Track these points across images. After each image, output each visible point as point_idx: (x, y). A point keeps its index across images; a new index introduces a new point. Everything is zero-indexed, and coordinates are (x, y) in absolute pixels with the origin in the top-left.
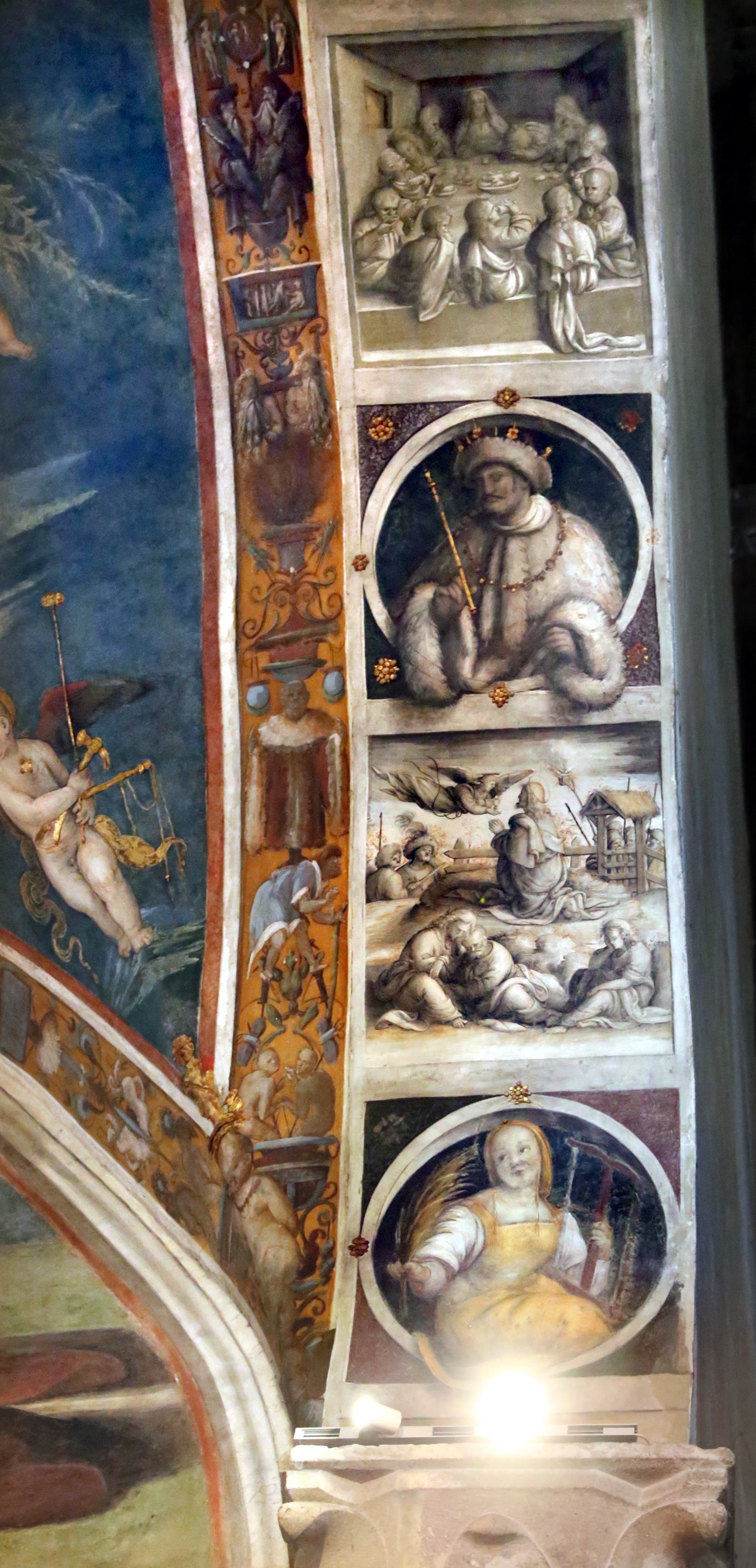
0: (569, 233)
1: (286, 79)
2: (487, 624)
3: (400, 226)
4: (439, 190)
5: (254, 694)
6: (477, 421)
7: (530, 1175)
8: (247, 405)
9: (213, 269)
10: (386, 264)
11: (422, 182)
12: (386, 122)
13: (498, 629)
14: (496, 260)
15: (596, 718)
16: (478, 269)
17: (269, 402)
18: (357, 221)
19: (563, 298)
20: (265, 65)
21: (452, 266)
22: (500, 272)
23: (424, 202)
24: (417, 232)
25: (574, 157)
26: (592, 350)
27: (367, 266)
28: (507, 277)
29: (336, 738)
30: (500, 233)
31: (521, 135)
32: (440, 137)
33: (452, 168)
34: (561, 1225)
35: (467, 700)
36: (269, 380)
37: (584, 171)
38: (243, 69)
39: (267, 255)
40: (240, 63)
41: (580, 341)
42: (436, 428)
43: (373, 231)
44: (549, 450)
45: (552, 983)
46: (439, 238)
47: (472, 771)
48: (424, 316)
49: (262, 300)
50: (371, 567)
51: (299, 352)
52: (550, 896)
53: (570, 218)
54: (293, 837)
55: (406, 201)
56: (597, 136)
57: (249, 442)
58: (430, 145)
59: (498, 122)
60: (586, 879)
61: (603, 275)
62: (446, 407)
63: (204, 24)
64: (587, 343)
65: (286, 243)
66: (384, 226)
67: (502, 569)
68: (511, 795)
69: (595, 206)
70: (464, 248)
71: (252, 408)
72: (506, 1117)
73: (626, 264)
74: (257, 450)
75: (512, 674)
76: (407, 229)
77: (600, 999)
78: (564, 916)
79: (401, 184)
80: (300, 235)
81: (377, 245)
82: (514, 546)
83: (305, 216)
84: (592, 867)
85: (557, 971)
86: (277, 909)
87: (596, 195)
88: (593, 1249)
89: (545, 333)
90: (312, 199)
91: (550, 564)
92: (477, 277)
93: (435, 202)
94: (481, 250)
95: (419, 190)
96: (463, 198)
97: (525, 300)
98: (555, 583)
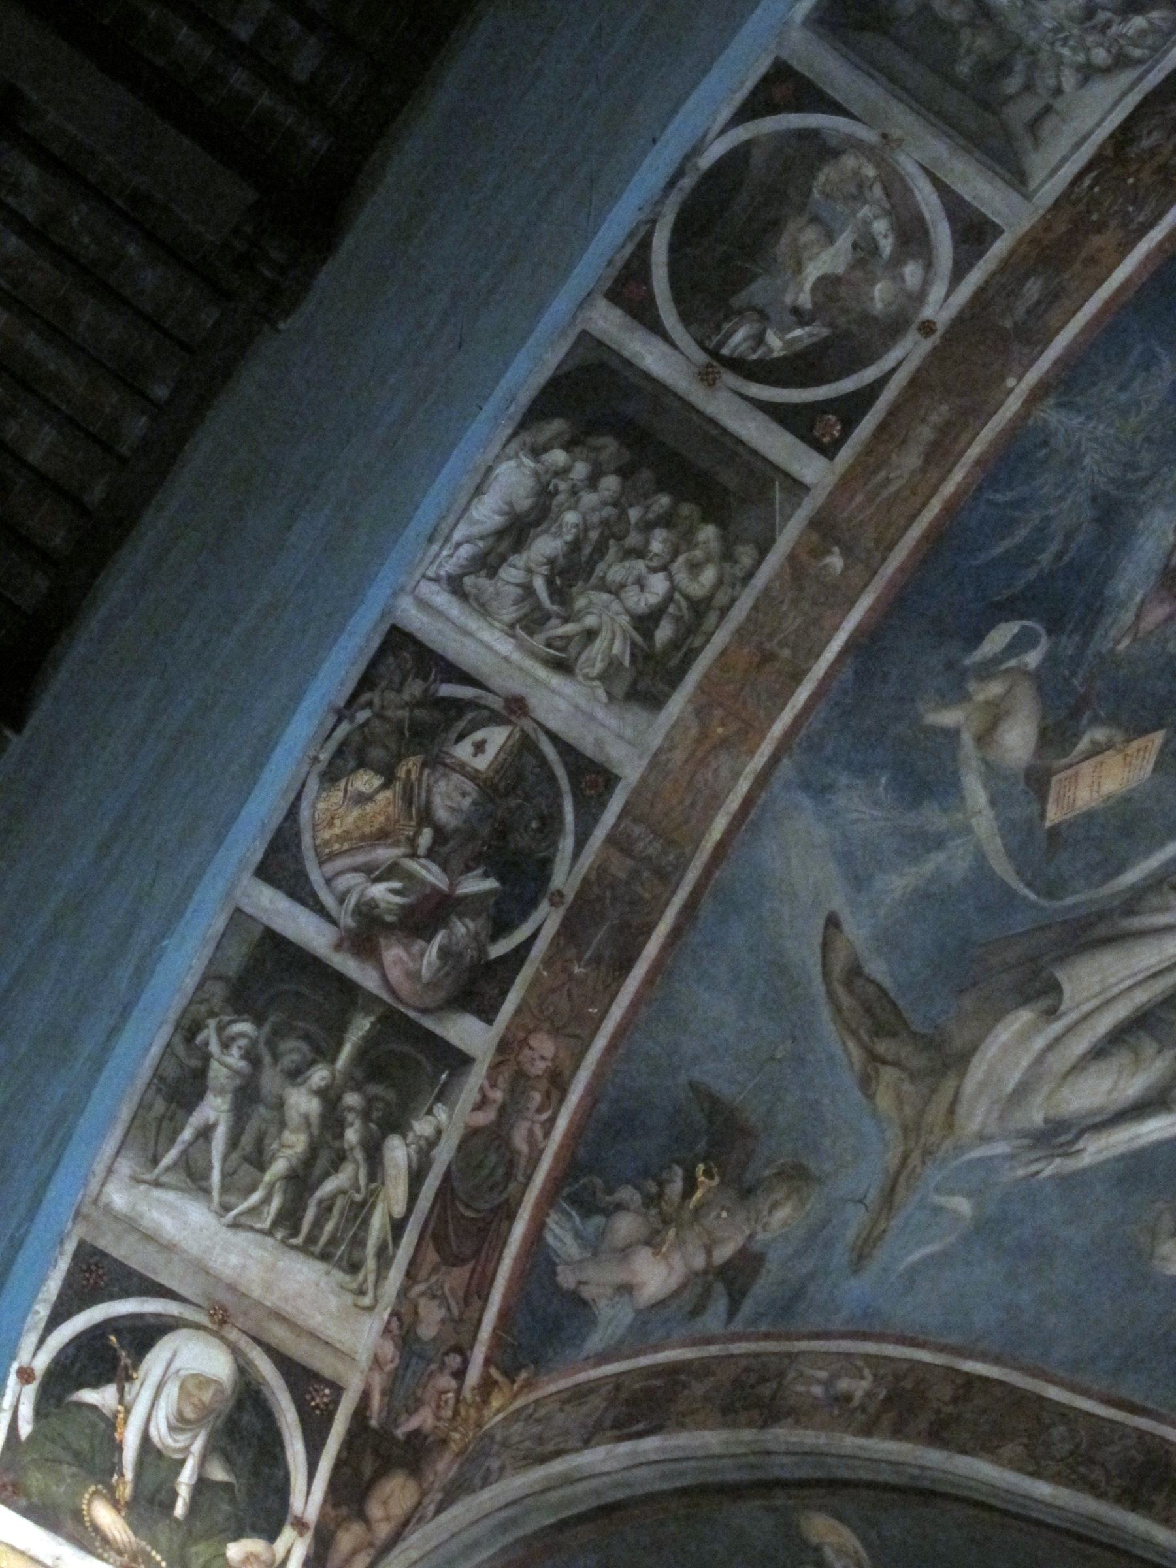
1: (1109, 152)
3: (1114, 30)
4: (1058, 29)
10: (1149, 15)
11: (1064, 45)
12: (1048, 109)
18: (1140, 62)
20: (1117, 171)
23: (1075, 31)
24: (1102, 16)
27: (1165, 26)
32: (1019, 65)
33: (1032, 37)
38: (1138, 180)
40: (1134, 185)
43: (1136, 46)
55: (1088, 44)
58: (1033, 66)
63: (1133, 226)
66: (1122, 42)
76: (1107, 25)
79: (1081, 58)
81: (1143, 33)
93: (1067, 23)
95: (1071, 43)
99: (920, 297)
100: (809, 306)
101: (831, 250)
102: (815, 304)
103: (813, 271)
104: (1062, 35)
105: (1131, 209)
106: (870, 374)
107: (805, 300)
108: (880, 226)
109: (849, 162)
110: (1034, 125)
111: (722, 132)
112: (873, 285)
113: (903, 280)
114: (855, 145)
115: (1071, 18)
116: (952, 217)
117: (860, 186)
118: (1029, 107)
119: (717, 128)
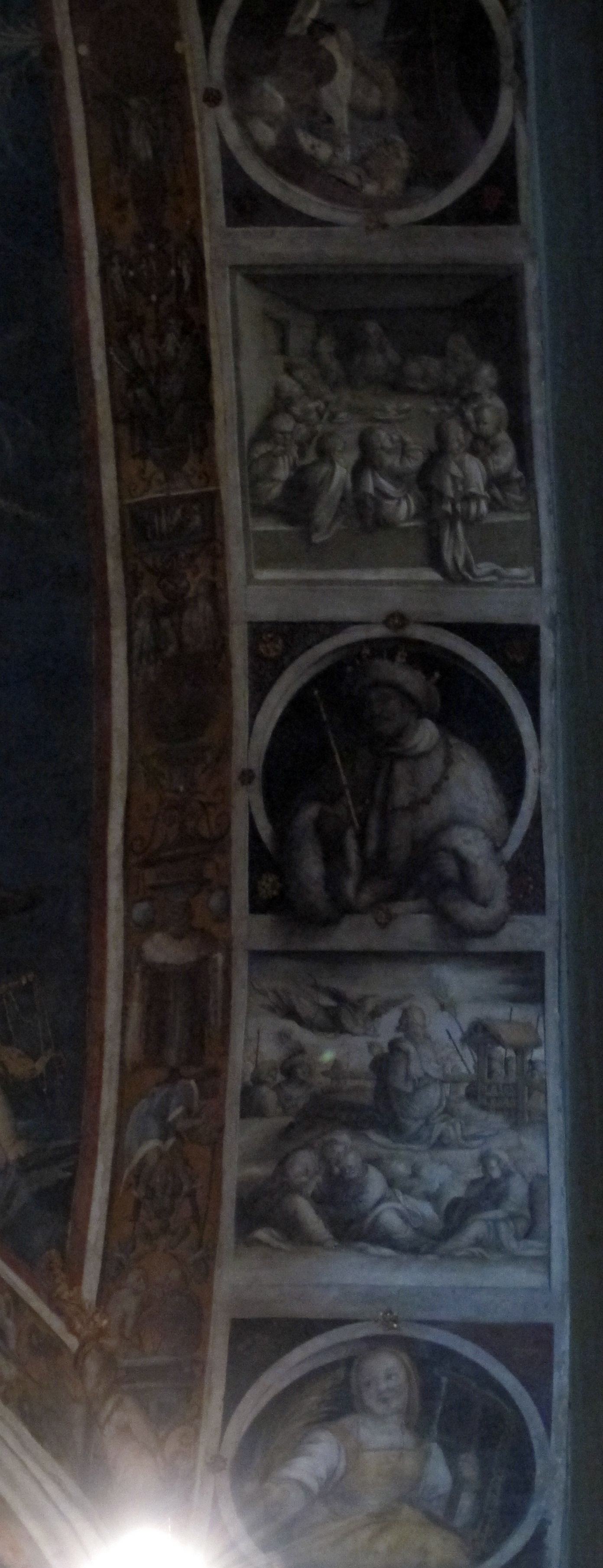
0: (461, 465)
2: (372, 845)
3: (294, 450)
4: (333, 417)
5: (140, 910)
6: (368, 642)
7: (396, 1403)
8: (143, 625)
9: (115, 491)
11: (317, 409)
12: (283, 350)
13: (382, 852)
14: (388, 487)
15: (480, 945)
16: (370, 495)
17: (165, 623)
19: (453, 527)
21: (345, 491)
22: (392, 498)
25: (465, 392)
26: (482, 580)
28: (399, 504)
29: (220, 957)
30: (392, 461)
31: (414, 368)
34: (427, 1455)
35: (348, 922)
36: (166, 601)
37: (475, 406)
38: (149, 303)
39: (168, 478)
41: (469, 569)
42: (326, 647)
44: (437, 675)
45: (427, 1209)
46: (332, 463)
47: (354, 992)
48: (317, 538)
49: (163, 523)
50: (257, 784)
51: (195, 574)
52: (428, 1122)
53: (462, 450)
54: (172, 1056)
55: (301, 426)
56: (487, 373)
57: (144, 662)
59: (393, 355)
60: (465, 1107)
61: (495, 505)
62: (335, 627)
63: (115, 260)
64: (477, 572)
65: (186, 468)
67: (389, 790)
68: (391, 1018)
69: (486, 439)
70: (357, 473)
71: (148, 628)
72: (374, 1343)
73: (516, 496)
74: (151, 670)
75: (395, 896)
76: (302, 453)
77: (476, 1229)
78: (441, 1143)
79: (297, 410)
80: (201, 461)
82: (400, 769)
83: (206, 443)
84: (471, 1095)
85: (432, 1198)
86: (153, 1127)
87: (488, 428)
88: (458, 1483)
89: (435, 560)
90: (213, 428)
91: (436, 788)
92: (370, 503)
94: (373, 475)
95: (314, 416)
96: (358, 426)
97: (416, 527)
98: (440, 807)
99: (242, 118)
100: (322, 42)
101: (345, 101)
102: (321, 48)
103: (344, 73)
104: (326, 416)
105: (131, 273)
106: (224, 24)
107: (331, 45)
108: (324, 152)
109: (393, 184)
110: (282, 329)
111: (513, 130)
112: (288, 100)
113: (270, 124)
114: (402, 201)
115: (331, 434)
116: (275, 202)
117: (368, 172)
118: (298, 340)
119: (520, 129)
